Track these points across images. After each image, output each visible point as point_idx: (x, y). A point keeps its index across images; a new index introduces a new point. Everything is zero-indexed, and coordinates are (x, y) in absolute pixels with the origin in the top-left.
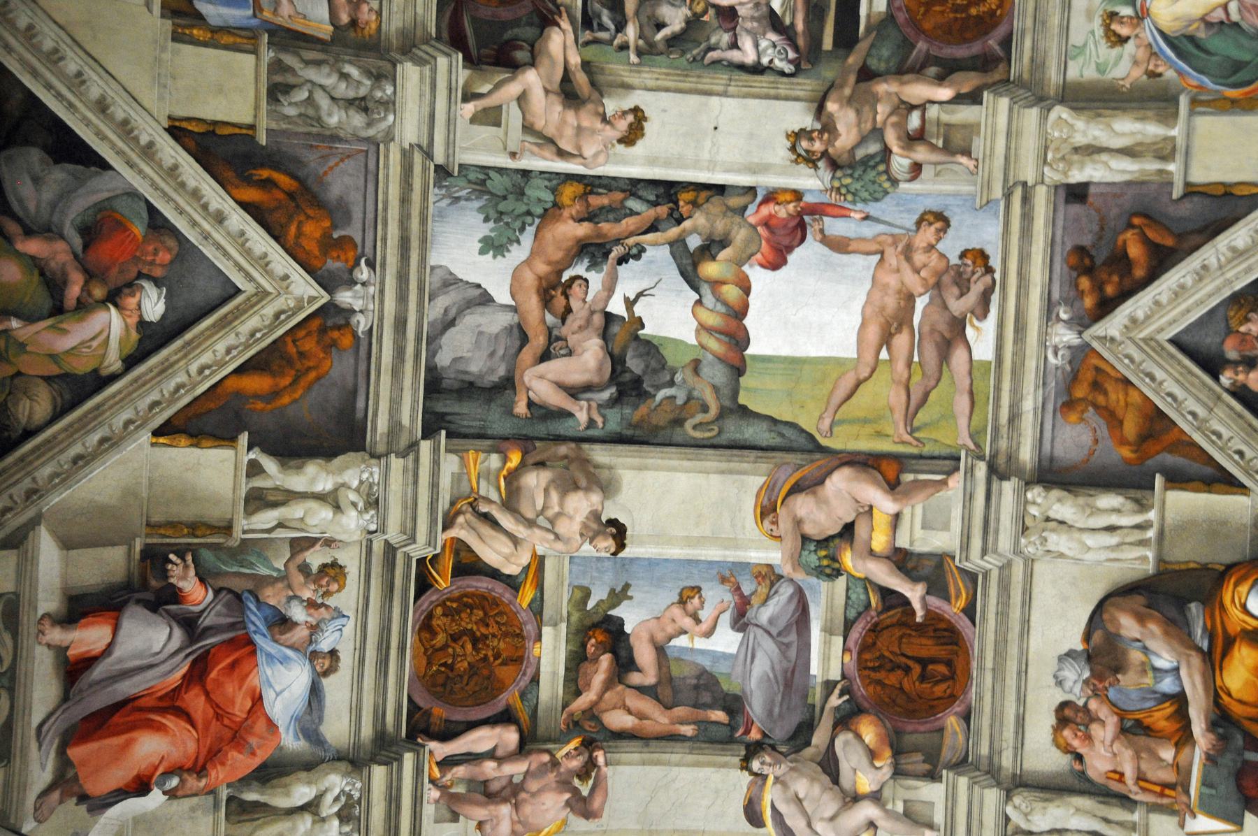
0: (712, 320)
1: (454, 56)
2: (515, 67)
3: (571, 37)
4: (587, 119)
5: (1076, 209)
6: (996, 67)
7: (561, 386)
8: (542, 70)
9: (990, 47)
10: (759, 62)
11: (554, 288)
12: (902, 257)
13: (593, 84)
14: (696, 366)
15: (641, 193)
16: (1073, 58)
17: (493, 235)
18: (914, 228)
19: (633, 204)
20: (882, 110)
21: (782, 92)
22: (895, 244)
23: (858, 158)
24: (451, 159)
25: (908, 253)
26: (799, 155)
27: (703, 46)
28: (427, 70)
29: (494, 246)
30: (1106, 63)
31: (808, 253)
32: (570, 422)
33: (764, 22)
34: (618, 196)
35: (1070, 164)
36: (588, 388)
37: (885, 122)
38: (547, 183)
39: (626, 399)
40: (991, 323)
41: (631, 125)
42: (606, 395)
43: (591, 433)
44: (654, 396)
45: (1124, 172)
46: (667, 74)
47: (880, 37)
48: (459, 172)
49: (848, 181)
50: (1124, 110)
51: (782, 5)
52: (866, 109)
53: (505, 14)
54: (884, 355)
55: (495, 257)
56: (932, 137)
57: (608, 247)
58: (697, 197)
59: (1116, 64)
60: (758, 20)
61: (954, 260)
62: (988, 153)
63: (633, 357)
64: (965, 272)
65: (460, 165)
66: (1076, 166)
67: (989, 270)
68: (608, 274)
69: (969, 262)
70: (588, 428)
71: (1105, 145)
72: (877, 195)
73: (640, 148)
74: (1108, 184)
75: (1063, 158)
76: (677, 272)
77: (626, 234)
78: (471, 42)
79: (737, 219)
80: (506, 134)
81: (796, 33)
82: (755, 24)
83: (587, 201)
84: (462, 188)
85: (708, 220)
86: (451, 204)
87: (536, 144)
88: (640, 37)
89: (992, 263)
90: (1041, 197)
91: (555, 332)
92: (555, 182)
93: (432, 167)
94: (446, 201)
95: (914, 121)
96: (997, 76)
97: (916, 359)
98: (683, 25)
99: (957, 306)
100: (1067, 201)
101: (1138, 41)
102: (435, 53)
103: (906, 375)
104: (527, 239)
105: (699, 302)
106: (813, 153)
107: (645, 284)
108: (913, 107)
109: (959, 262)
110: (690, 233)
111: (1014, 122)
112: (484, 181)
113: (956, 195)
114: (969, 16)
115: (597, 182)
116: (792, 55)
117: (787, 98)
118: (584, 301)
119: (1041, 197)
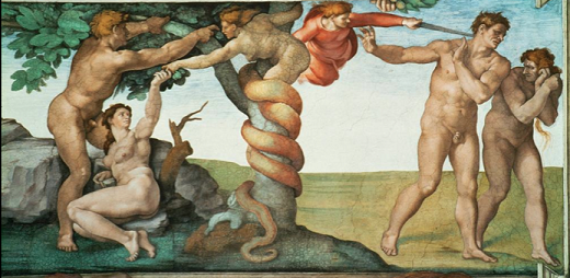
0: (264, 141)
7: (107, 217)
12: (460, 63)
14: (249, 188)
15: (181, 17)
17: (26, 69)
18: (471, 32)
19: (173, 28)
22: (451, 50)
25: (466, 58)
29: (26, 81)
31: (361, 65)
32: (120, 253)
36: (137, 216)
38: (81, 14)
39: (178, 226)
40: (558, 129)
42: (156, 223)
43: (141, 262)
44: (208, 221)
54: (447, 166)
55: (29, 91)
57: (149, 73)
58: (240, 17)
61: (516, 63)
63: (183, 183)
64: (528, 74)
67: (555, 71)
68: (151, 101)
69: (533, 64)
70: (138, 258)
77: (168, 59)
79: (284, 36)
83: (125, 28)
85: (253, 39)
89: (557, 63)
91: (98, 163)
92: (89, 12)
97: (482, 169)
99: (521, 111)
103: (472, 187)
104: (64, 70)
105: (248, 123)
109: (522, 65)
112: (15, 16)
115: (135, 9)
118: (127, 129)
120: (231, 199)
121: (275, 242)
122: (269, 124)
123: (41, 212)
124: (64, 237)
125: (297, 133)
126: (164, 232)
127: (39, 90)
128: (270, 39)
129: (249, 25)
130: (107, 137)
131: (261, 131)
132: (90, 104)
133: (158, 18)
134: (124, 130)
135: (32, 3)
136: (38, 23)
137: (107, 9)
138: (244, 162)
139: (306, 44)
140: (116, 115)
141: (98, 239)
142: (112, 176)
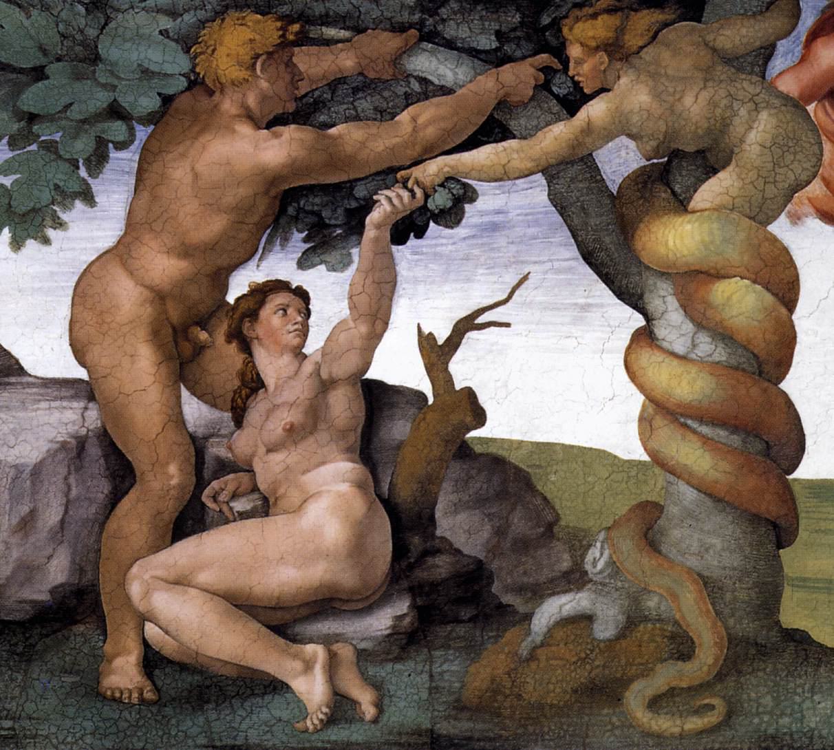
11: (203, 323)
15: (450, 31)
32: (276, 708)
38: (165, 23)
39: (442, 631)
42: (381, 622)
44: (528, 617)
55: (17, 244)
57: (360, 191)
58: (621, 31)
63: (456, 508)
68: (365, 272)
70: (331, 721)
76: (574, 252)
77: (414, 153)
79: (747, 86)
83: (289, 64)
85: (657, 95)
91: (216, 450)
92: (189, 18)
105: (645, 337)
107: (479, 295)
110: (609, 136)
120: (594, 553)
121: (720, 677)
122: (704, 340)
123: (53, 591)
124: (118, 662)
125: (784, 364)
126: (403, 648)
127: (46, 241)
128: (705, 95)
129: (648, 54)
130: (242, 375)
131: (683, 358)
132: (192, 280)
134: (287, 359)
136: (45, 52)
138: (631, 448)
139: (811, 108)
140: (265, 312)
141: (217, 669)
142: (255, 489)
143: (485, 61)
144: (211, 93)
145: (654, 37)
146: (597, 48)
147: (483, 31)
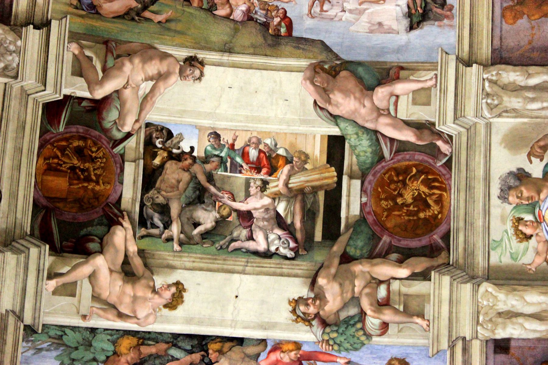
1: (43, 247)
2: (87, 254)
3: (130, 232)
4: (141, 291)
5: (502, 358)
6: (440, 254)
8: (108, 256)
9: (434, 240)
10: (268, 250)
13: (146, 265)
15: (180, 344)
16: (495, 249)
19: (174, 352)
20: (359, 284)
21: (285, 271)
23: (342, 318)
24: (37, 321)
26: (298, 316)
27: (228, 238)
28: (22, 257)
30: (517, 253)
33: (272, 222)
34: (163, 346)
35: (496, 325)
37: (361, 293)
38: (109, 337)
41: (173, 295)
45: (535, 331)
46: (201, 258)
47: (356, 232)
48: (42, 330)
49: (334, 335)
50: (532, 286)
51: (285, 210)
52: (347, 283)
53: (82, 218)
56: (395, 304)
58: (222, 347)
59: (524, 254)
60: (267, 220)
62: (436, 315)
65: (43, 325)
66: (500, 326)
71: (520, 311)
72: (355, 346)
73: (180, 311)
74: (523, 339)
75: (491, 320)
78: (56, 236)
80: (79, 302)
81: (295, 229)
82: (266, 223)
83: (139, 350)
84: (44, 342)
86: (35, 354)
87: (101, 309)
88: (181, 233)
90: (476, 348)
92: (115, 337)
93: (22, 327)
94: (31, 352)
95: (382, 292)
96: (440, 260)
98: (214, 223)
100: (495, 352)
101: (538, 238)
102: (29, 245)
106: (309, 314)
108: (381, 282)
111: (455, 293)
112: (62, 336)
113: (414, 346)
114: (419, 219)
115: (147, 336)
116: (292, 245)
117: (289, 275)
119: (476, 348)
133: (164, 344)
135: (75, 327)
137: (127, 334)
143: (188, 353)
144: (119, 356)
145: (230, 349)
146: (216, 351)
147: (188, 345)
